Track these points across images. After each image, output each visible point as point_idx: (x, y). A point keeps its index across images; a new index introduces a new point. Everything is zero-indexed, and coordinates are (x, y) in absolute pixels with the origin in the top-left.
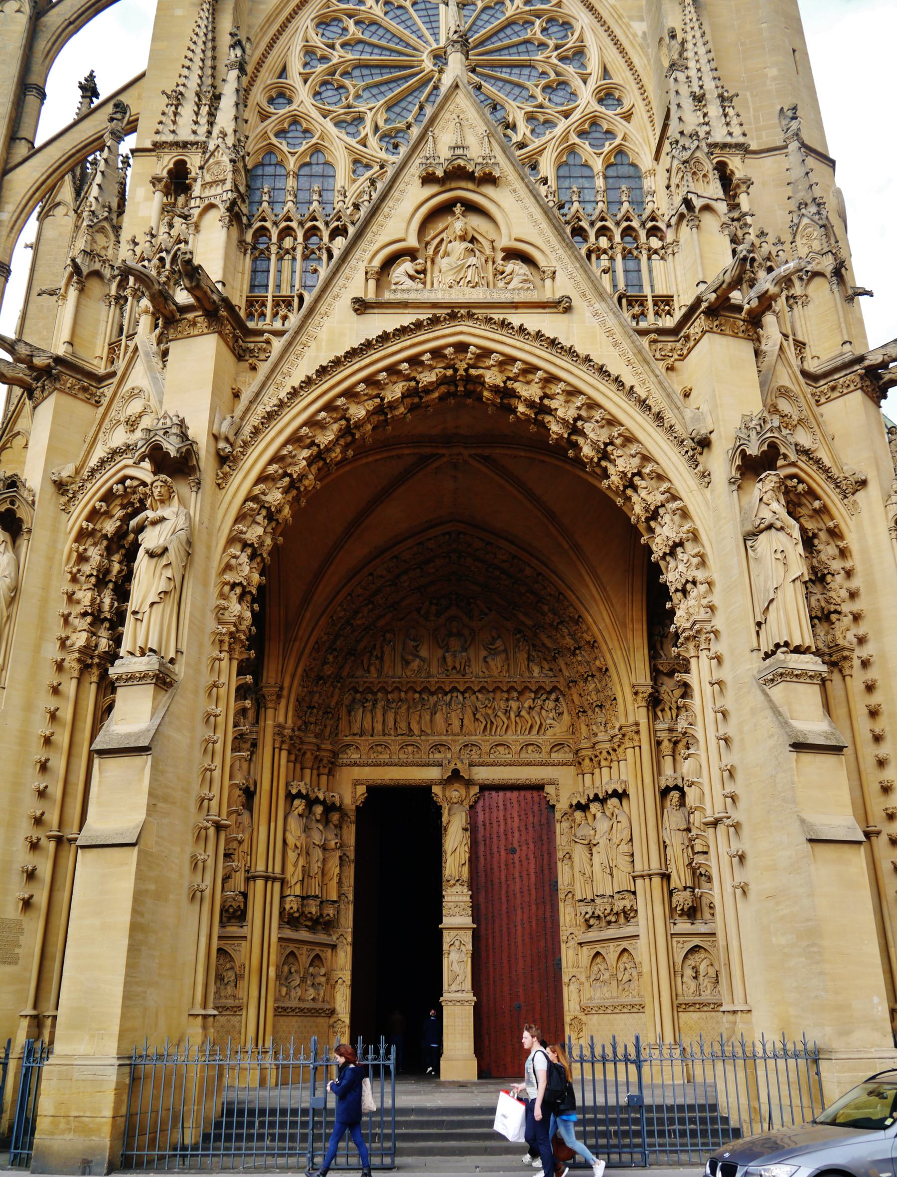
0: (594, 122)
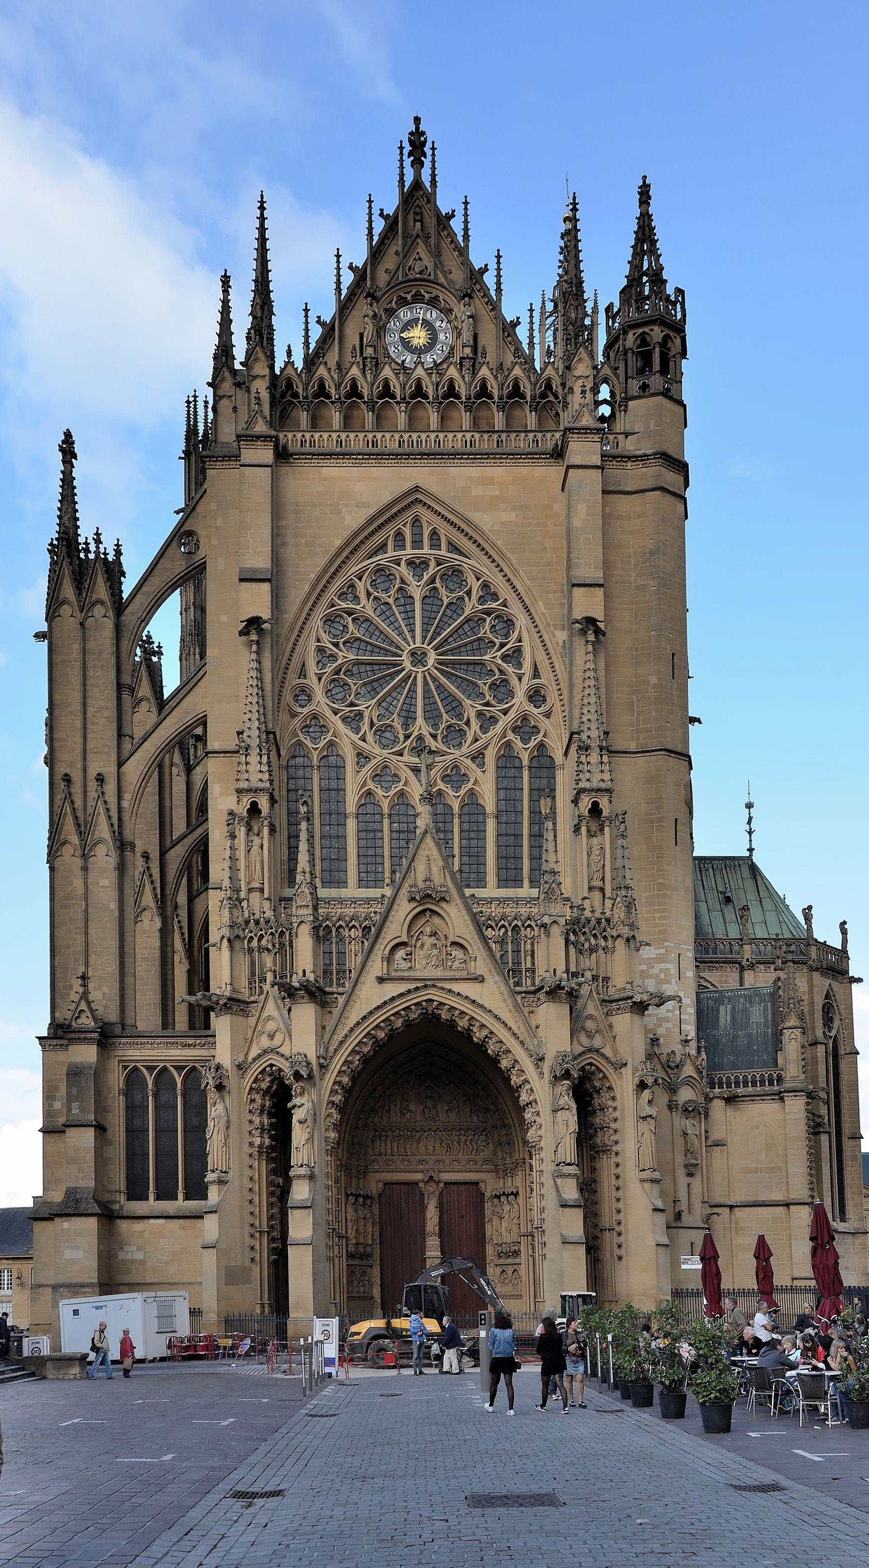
0: (525, 718)
